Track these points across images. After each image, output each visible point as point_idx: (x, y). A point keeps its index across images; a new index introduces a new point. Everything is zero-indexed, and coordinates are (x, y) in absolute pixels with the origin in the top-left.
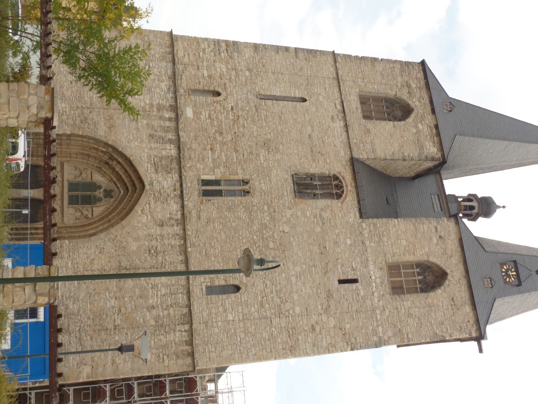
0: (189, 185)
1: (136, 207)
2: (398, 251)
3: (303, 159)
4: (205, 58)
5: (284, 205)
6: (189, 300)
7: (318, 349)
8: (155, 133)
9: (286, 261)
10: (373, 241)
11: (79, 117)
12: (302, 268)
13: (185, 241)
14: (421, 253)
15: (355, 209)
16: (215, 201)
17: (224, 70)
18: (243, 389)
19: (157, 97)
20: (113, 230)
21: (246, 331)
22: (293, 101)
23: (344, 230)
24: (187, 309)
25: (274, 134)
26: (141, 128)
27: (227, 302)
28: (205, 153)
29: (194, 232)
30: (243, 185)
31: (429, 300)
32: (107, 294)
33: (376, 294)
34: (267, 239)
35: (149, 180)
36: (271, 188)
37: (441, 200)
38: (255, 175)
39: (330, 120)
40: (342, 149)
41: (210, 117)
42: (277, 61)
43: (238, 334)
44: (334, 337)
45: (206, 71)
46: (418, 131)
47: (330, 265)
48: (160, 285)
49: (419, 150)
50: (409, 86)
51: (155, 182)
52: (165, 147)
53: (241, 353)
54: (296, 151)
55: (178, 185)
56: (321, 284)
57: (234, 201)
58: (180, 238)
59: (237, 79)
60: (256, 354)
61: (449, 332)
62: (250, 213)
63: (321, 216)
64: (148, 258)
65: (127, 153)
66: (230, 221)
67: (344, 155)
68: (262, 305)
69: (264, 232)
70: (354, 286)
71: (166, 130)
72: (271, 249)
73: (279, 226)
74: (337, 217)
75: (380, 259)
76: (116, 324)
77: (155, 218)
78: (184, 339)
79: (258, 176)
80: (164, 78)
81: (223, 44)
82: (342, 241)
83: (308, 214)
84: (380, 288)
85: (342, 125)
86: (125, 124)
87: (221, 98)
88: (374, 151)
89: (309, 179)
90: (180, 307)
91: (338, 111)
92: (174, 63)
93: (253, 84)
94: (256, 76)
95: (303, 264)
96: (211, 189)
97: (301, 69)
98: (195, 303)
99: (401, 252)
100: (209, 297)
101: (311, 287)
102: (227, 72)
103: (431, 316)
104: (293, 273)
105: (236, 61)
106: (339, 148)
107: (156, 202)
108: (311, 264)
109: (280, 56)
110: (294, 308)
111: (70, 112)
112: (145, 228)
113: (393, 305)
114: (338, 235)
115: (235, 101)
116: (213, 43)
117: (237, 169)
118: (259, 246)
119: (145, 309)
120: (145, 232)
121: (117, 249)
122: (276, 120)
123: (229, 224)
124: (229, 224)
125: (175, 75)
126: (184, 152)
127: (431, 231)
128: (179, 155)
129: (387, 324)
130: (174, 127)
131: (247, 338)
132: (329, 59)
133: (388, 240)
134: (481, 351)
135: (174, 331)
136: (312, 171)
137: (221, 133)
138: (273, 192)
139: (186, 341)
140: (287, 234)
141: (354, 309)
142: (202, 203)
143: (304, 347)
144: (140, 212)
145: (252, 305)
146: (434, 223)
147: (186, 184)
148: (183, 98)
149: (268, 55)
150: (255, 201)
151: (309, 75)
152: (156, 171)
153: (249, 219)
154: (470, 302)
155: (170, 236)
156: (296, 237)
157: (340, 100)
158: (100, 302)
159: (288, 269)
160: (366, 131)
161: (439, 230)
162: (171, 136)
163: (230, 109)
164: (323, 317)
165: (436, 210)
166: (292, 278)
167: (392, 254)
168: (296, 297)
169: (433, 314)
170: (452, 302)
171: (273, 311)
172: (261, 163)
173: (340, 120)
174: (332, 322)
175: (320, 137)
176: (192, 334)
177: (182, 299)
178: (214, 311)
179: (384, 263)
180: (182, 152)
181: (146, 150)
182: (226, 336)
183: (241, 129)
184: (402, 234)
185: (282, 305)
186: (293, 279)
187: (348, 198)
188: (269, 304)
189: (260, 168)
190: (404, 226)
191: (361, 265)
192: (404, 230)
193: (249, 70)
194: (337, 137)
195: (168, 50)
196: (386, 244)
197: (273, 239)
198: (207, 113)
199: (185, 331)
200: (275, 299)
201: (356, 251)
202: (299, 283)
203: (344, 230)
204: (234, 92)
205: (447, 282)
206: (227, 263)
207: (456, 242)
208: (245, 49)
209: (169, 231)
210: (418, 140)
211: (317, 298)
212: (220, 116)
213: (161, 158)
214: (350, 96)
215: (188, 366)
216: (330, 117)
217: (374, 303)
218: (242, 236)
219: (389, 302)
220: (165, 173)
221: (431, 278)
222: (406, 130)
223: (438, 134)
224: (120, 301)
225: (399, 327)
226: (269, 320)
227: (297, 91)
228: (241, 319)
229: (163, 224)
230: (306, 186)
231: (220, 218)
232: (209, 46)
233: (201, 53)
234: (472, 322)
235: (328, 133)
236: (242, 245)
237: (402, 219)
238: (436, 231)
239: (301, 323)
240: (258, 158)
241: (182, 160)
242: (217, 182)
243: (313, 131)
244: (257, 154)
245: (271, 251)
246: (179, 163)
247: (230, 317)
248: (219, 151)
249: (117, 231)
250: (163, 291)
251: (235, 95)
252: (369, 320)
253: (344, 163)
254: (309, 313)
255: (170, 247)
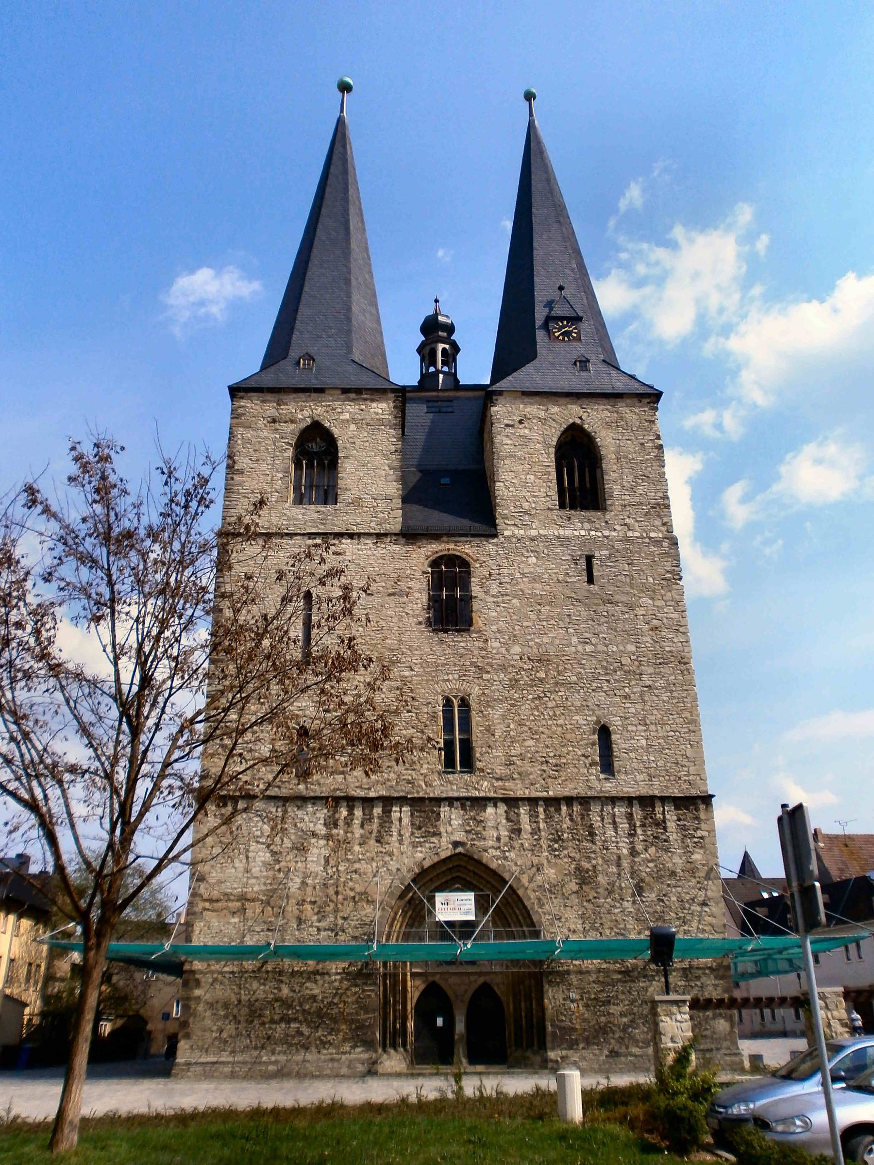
5: (481, 649)
27: (623, 746)
33: (606, 533)
44: (666, 601)
46: (353, 420)
62: (495, 700)
118: (543, 692)
119: (636, 860)
124: (512, 733)
136: (424, 598)
141: (626, 567)
143: (680, 644)
150: (476, 691)
161: (510, 423)
171: (633, 683)
172: (416, 676)
187: (467, 551)
200: (616, 677)
202: (593, 640)
222: (352, 440)
223: (359, 391)
230: (450, 610)
235: (362, 564)
238: (512, 426)
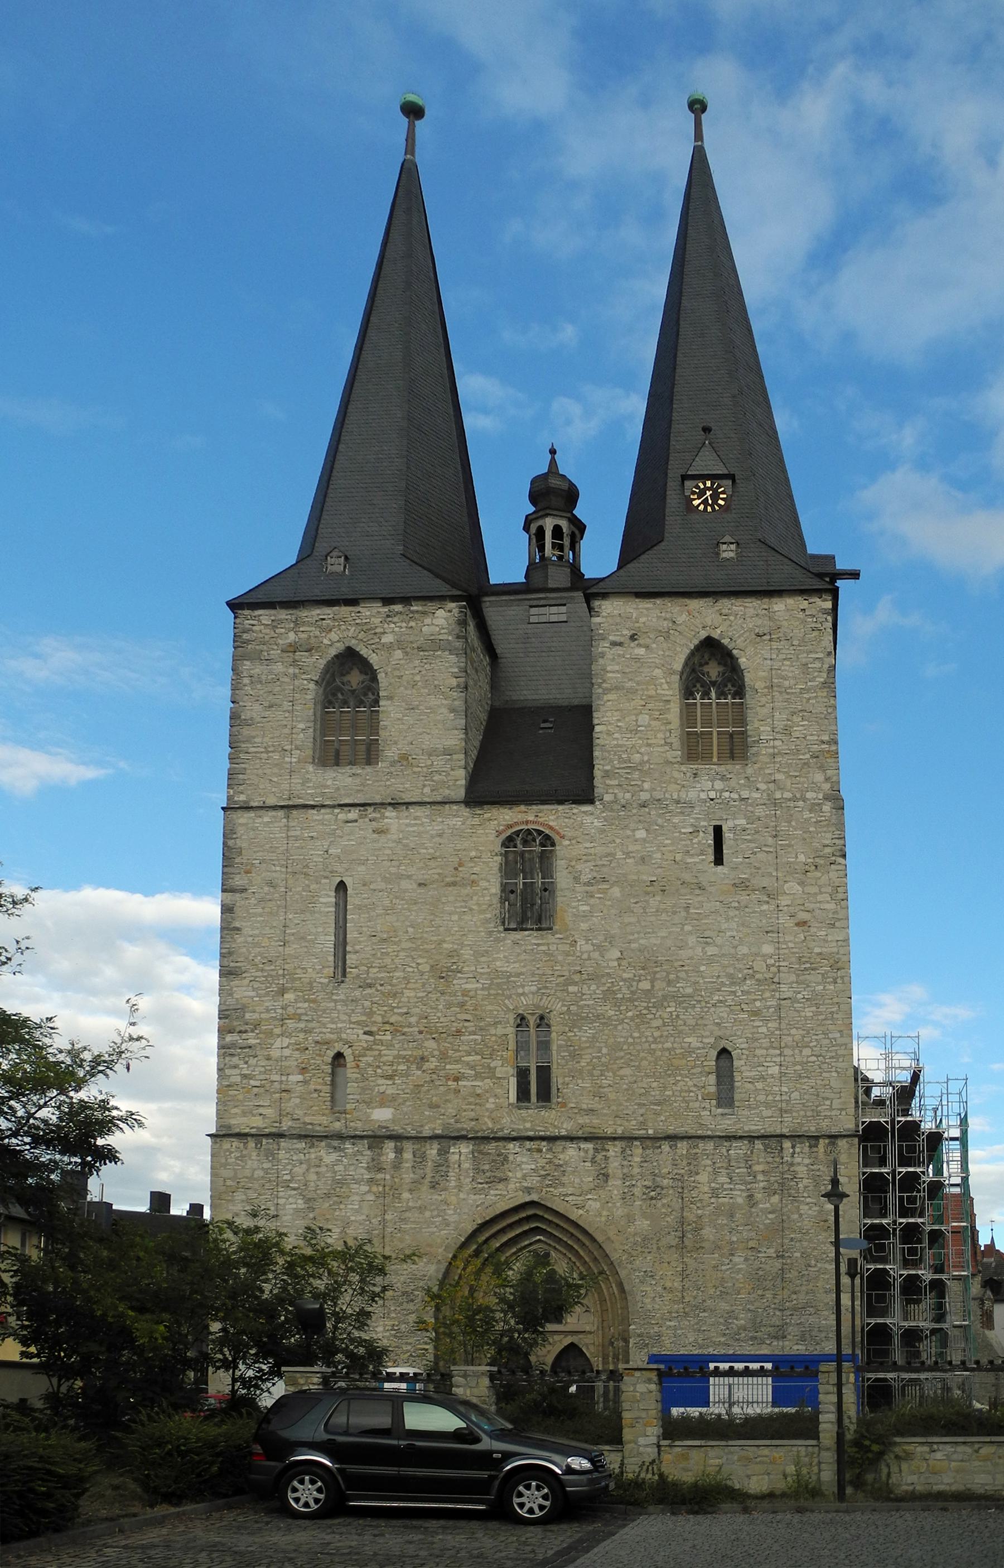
0: (528, 1125)
1: (573, 1217)
2: (660, 735)
3: (472, 904)
4: (262, 1077)
6: (741, 1137)
7: (840, 920)
8: (428, 1179)
9: (677, 960)
10: (639, 783)
11: (402, 1304)
12: (690, 933)
13: (636, 1138)
14: (665, 686)
15: (575, 811)
16: (560, 1081)
17: (286, 1041)
18: (888, 1038)
19: (355, 1170)
20: (614, 1257)
21: (800, 1045)
22: (346, 910)
23: (618, 841)
24: (756, 1142)
25: (420, 956)
26: (420, 1202)
27: (748, 1074)
28: (463, 1092)
29: (619, 1123)
30: (528, 1026)
31: (759, 685)
32: (724, 1268)
33: (745, 794)
34: (633, 993)
35: (521, 1193)
36: (533, 975)
37: (542, 602)
38: (506, 1001)
39: (383, 838)
40: (448, 821)
41: (390, 1077)
42: (257, 932)
43: (805, 1060)
44: (820, 887)
45: (290, 1077)
46: (400, 644)
47: (687, 877)
48: (713, 1185)
49: (444, 650)
50: (293, 648)
51: (526, 1185)
52: (454, 1164)
53: (836, 1057)
54: (455, 917)
55: (528, 1144)
56: (721, 899)
57: (559, 1046)
58: (630, 1147)
59: (304, 1018)
60: (840, 1031)
61: (820, 655)
62: (583, 1018)
63: (589, 884)
64: (665, 1201)
65: (470, 1228)
66: (599, 1057)
67: (460, 818)
68: (756, 1013)
69: (620, 996)
70: (727, 835)
71: (420, 1158)
72: (653, 986)
73: (608, 967)
74: (592, 851)
75: (676, 774)
76: (774, 1255)
77: (592, 1186)
78: (807, 1149)
79: (509, 997)
80: (313, 1156)
81: (229, 1038)
82: (639, 847)
83: (586, 908)
84: (733, 783)
85: (394, 814)
86: (411, 1228)
87: (347, 1052)
88: (448, 752)
89: (512, 896)
90: (752, 1153)
91: (361, 817)
92: (281, 1135)
93: (312, 988)
94: (294, 980)
95: (682, 929)
96: (536, 1086)
97: (271, 884)
98: (746, 1129)
99: (663, 728)
100: (737, 1104)
101: (727, 919)
102: (290, 1036)
103: (790, 688)
104: (699, 950)
105: (263, 1016)
106: (446, 827)
107: (563, 1185)
108: (683, 914)
109: (248, 928)
110: (763, 956)
111: (393, 1318)
112: (610, 1205)
113: (767, 763)
114: (628, 855)
115: (352, 1026)
116: (227, 1058)
117: (495, 1035)
118: (647, 1008)
119: (753, 1210)
120: (618, 1204)
121: (647, 1250)
122: (389, 950)
123: (603, 1060)
124: (603, 1060)
125: (306, 1136)
126: (463, 1129)
127: (619, 655)
128: (471, 1139)
129: (802, 779)
130: (413, 1144)
131: (811, 1044)
132: (242, 821)
133: (638, 752)
134: (855, 575)
135: (792, 1164)
136: (495, 889)
137: (422, 1058)
138: (541, 972)
139: (810, 1147)
140: (625, 953)
141: (770, 841)
142: (564, 1105)
143: (834, 944)
144: (581, 1212)
145: (755, 1030)
146: (603, 646)
147: (527, 1130)
148: (352, 1124)
149: (244, 950)
150: (559, 1007)
151: (284, 870)
152: (504, 1180)
153: (594, 1021)
154: (766, 600)
155: (625, 1163)
156: (631, 937)
157: (337, 811)
158: (737, 1280)
159: (691, 958)
160: (405, 763)
161: (617, 639)
162: (432, 1151)
163: (371, 1038)
164: (784, 903)
165: (563, 618)
166: (709, 953)
167: (667, 748)
168: (744, 950)
169: (787, 683)
170: (764, 638)
171: (767, 994)
172: (483, 989)
173: (383, 817)
174: (793, 887)
175: (421, 865)
176: (799, 1136)
177: (738, 1149)
178: (762, 1098)
179: (683, 768)
180: (464, 1133)
181: (462, 1196)
182: (806, 1080)
183: (413, 1020)
184: (627, 719)
185: (757, 976)
186: (711, 950)
187: (551, 823)
188: (755, 1000)
189: (492, 992)
190: (609, 714)
191: (688, 815)
192: (617, 715)
193: (282, 991)
194: (421, 828)
195: (251, 1144)
196: (646, 758)
197: (633, 980)
198: (381, 1081)
199: (793, 1147)
200: (746, 988)
201: (660, 821)
202: (719, 941)
203: (618, 841)
204: (334, 1026)
205: (725, 641)
206: (677, 1069)
207: (645, 604)
208: (235, 996)
209: (616, 1164)
210: (420, 649)
211: (747, 910)
212: (385, 1058)
213: (478, 1170)
214: (328, 787)
215: (852, 1145)
216: (375, 835)
217: (762, 802)
218: (627, 1038)
219: (760, 769)
220: (506, 1166)
221: (713, 670)
223: (406, 600)
224: (737, 1249)
225: (808, 756)
226: (782, 1002)
227: (322, 900)
228: (778, 1052)
229: (604, 1174)
230: (528, 902)
231: (592, 1075)
232: (235, 1067)
233: (252, 1083)
234: (805, 604)
236: (644, 1040)
237: (595, 715)
238: (621, 644)
239: (791, 945)
240: (471, 994)
241: (479, 1134)
242: (522, 1075)
243: (409, 877)
244: (463, 995)
245: (657, 987)
246: (486, 1139)
247: (775, 1070)
248: (459, 1066)
249: (615, 1250)
250: (723, 1179)
251: (340, 1025)
252: (791, 815)
253: (476, 821)
254: (775, 929)
255: (645, 1165)
